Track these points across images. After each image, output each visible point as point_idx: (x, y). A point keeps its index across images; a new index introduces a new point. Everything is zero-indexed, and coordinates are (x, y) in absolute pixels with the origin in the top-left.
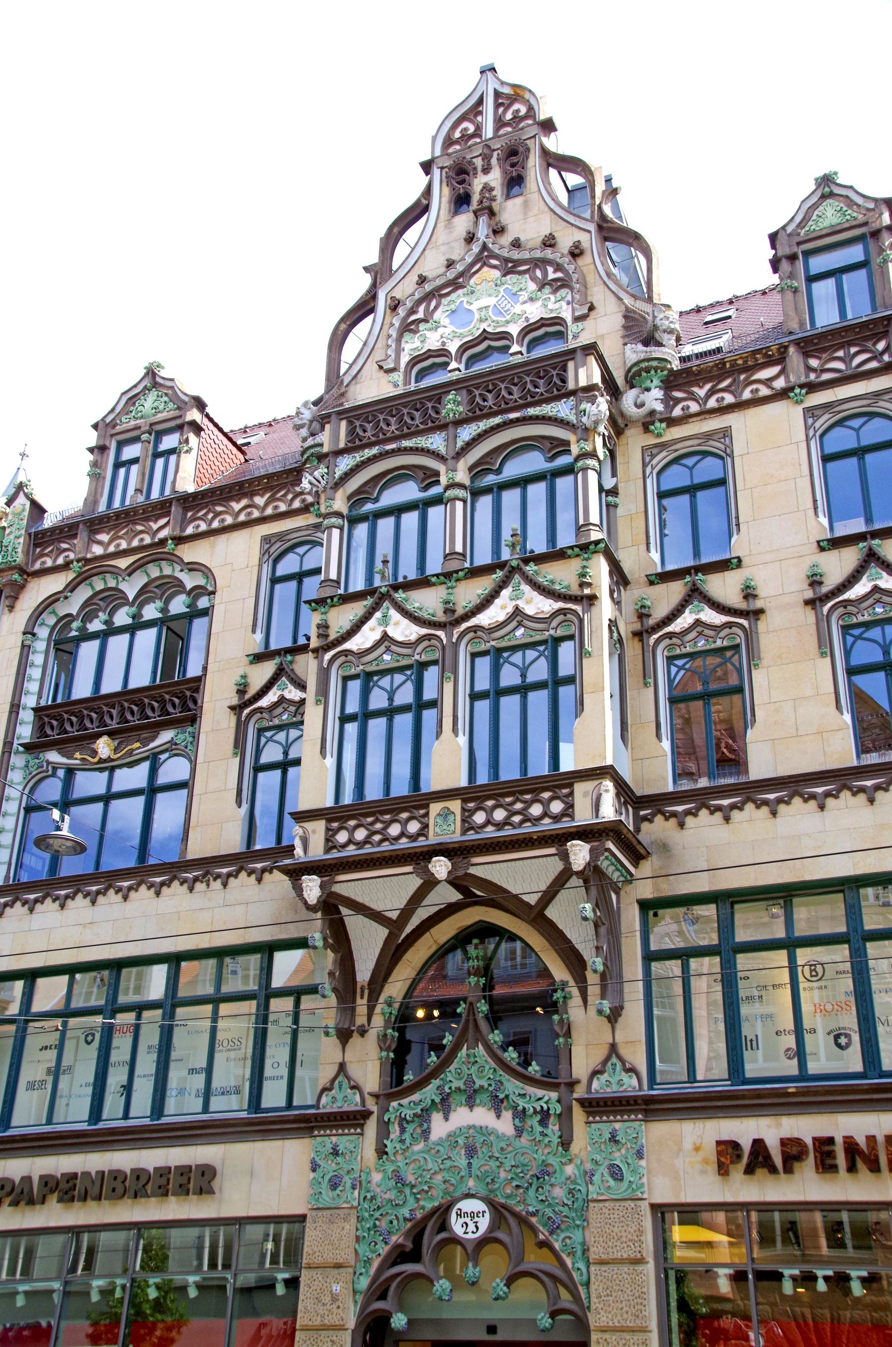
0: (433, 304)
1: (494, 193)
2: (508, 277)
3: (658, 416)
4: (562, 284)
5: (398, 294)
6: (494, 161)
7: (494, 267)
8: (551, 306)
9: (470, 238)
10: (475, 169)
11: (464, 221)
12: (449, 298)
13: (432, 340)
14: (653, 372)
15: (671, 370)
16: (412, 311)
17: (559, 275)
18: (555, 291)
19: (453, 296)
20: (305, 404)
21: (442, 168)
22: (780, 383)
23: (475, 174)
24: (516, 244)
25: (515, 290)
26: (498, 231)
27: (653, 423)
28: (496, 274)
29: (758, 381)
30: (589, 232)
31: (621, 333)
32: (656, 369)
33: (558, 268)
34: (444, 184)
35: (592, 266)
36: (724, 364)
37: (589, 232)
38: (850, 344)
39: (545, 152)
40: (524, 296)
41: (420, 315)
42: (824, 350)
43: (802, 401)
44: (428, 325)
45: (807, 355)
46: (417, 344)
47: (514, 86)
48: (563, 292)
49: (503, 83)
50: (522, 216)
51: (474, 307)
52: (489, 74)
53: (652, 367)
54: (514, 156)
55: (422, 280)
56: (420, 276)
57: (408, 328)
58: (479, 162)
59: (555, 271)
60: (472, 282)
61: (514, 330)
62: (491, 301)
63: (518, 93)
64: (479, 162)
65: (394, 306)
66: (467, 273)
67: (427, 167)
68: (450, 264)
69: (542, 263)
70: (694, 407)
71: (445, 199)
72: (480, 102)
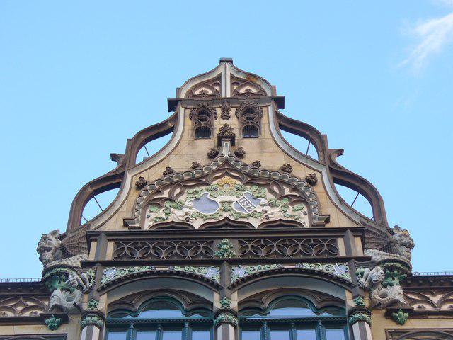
0: (178, 191)
1: (234, 132)
2: (248, 187)
4: (302, 200)
5: (146, 176)
6: (233, 111)
8: (289, 212)
9: (213, 155)
10: (216, 113)
11: (206, 145)
12: (193, 190)
13: (177, 216)
14: (396, 272)
16: (159, 192)
18: (292, 204)
19: (198, 189)
20: (54, 233)
21: (186, 108)
23: (216, 118)
25: (255, 196)
26: (240, 155)
28: (238, 182)
30: (320, 172)
32: (399, 269)
33: (295, 189)
34: (187, 119)
35: (325, 194)
37: (320, 172)
39: (279, 117)
41: (166, 194)
44: (174, 204)
46: (163, 215)
47: (249, 75)
49: (239, 71)
50: (258, 151)
51: (218, 199)
52: (228, 65)
53: (396, 267)
55: (169, 171)
56: (168, 169)
57: (157, 203)
58: (219, 112)
60: (215, 182)
62: (234, 199)
63: (251, 79)
64: (219, 112)
65: (141, 185)
67: (172, 105)
68: (195, 166)
69: (280, 183)
72: (219, 77)
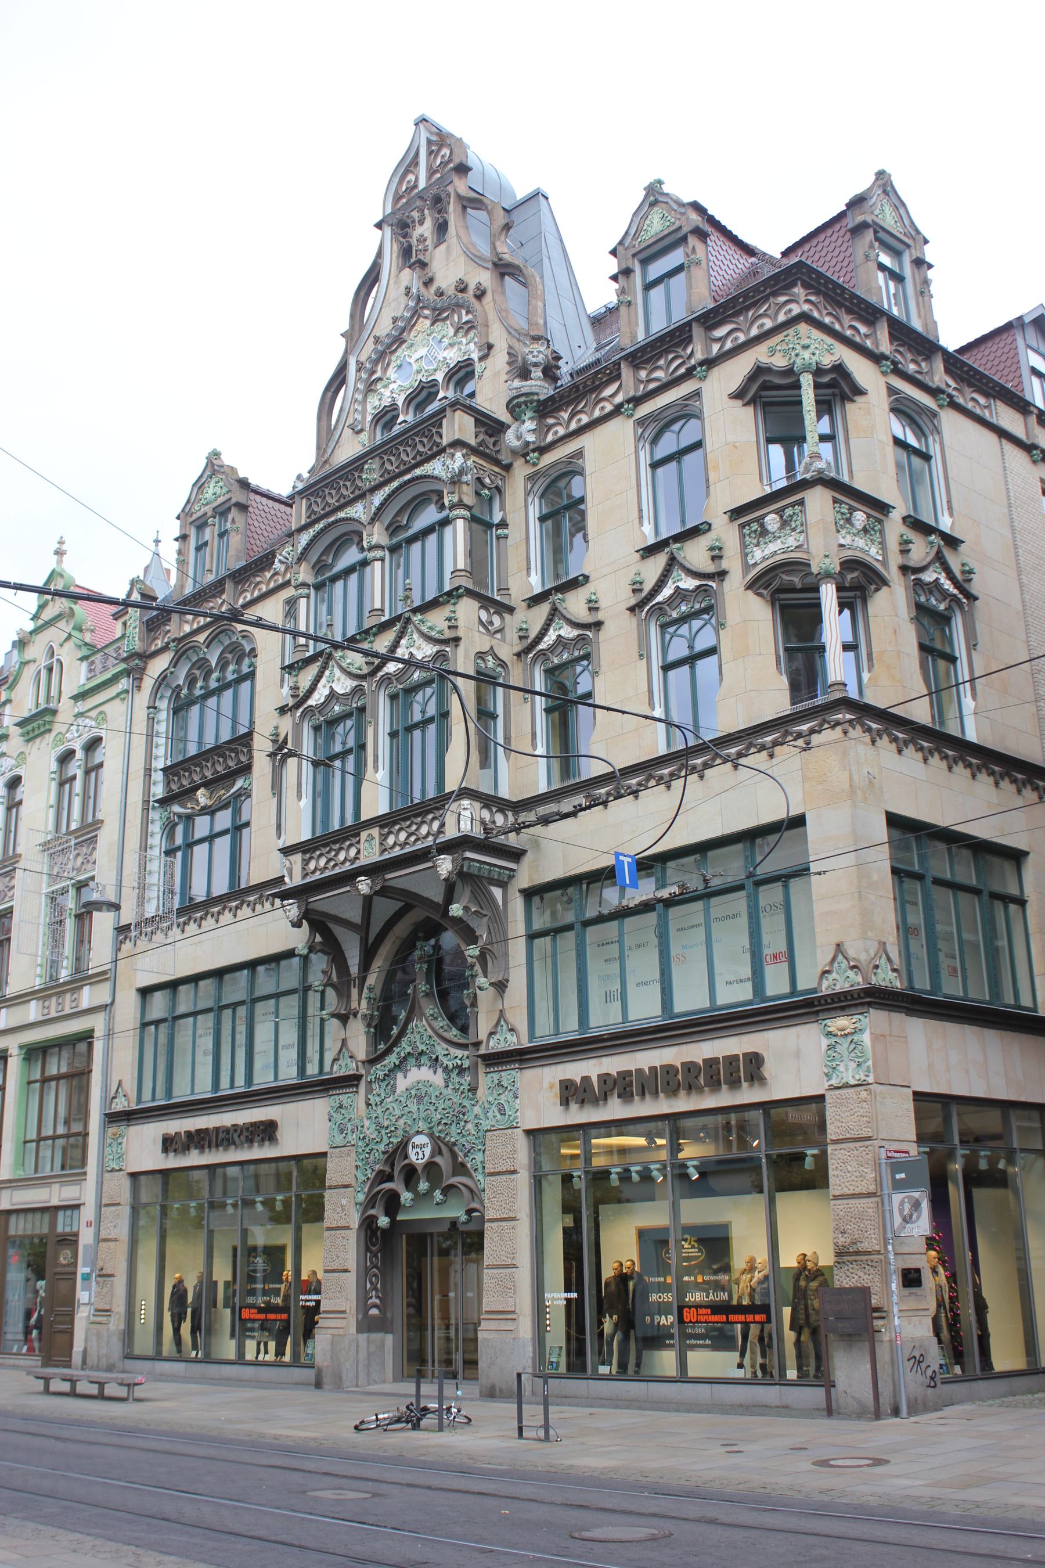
1: (427, 243)
3: (532, 447)
6: (426, 212)
7: (426, 317)
10: (413, 221)
15: (539, 401)
17: (470, 317)
21: (392, 225)
22: (619, 399)
24: (440, 294)
25: (439, 337)
27: (527, 454)
29: (604, 399)
31: (507, 368)
36: (577, 387)
38: (667, 351)
40: (446, 341)
42: (647, 362)
43: (632, 415)
45: (637, 367)
48: (471, 334)
54: (438, 203)
58: (415, 215)
59: (468, 312)
61: (440, 377)
66: (409, 325)
69: (457, 306)
70: (561, 431)
71: (395, 255)
